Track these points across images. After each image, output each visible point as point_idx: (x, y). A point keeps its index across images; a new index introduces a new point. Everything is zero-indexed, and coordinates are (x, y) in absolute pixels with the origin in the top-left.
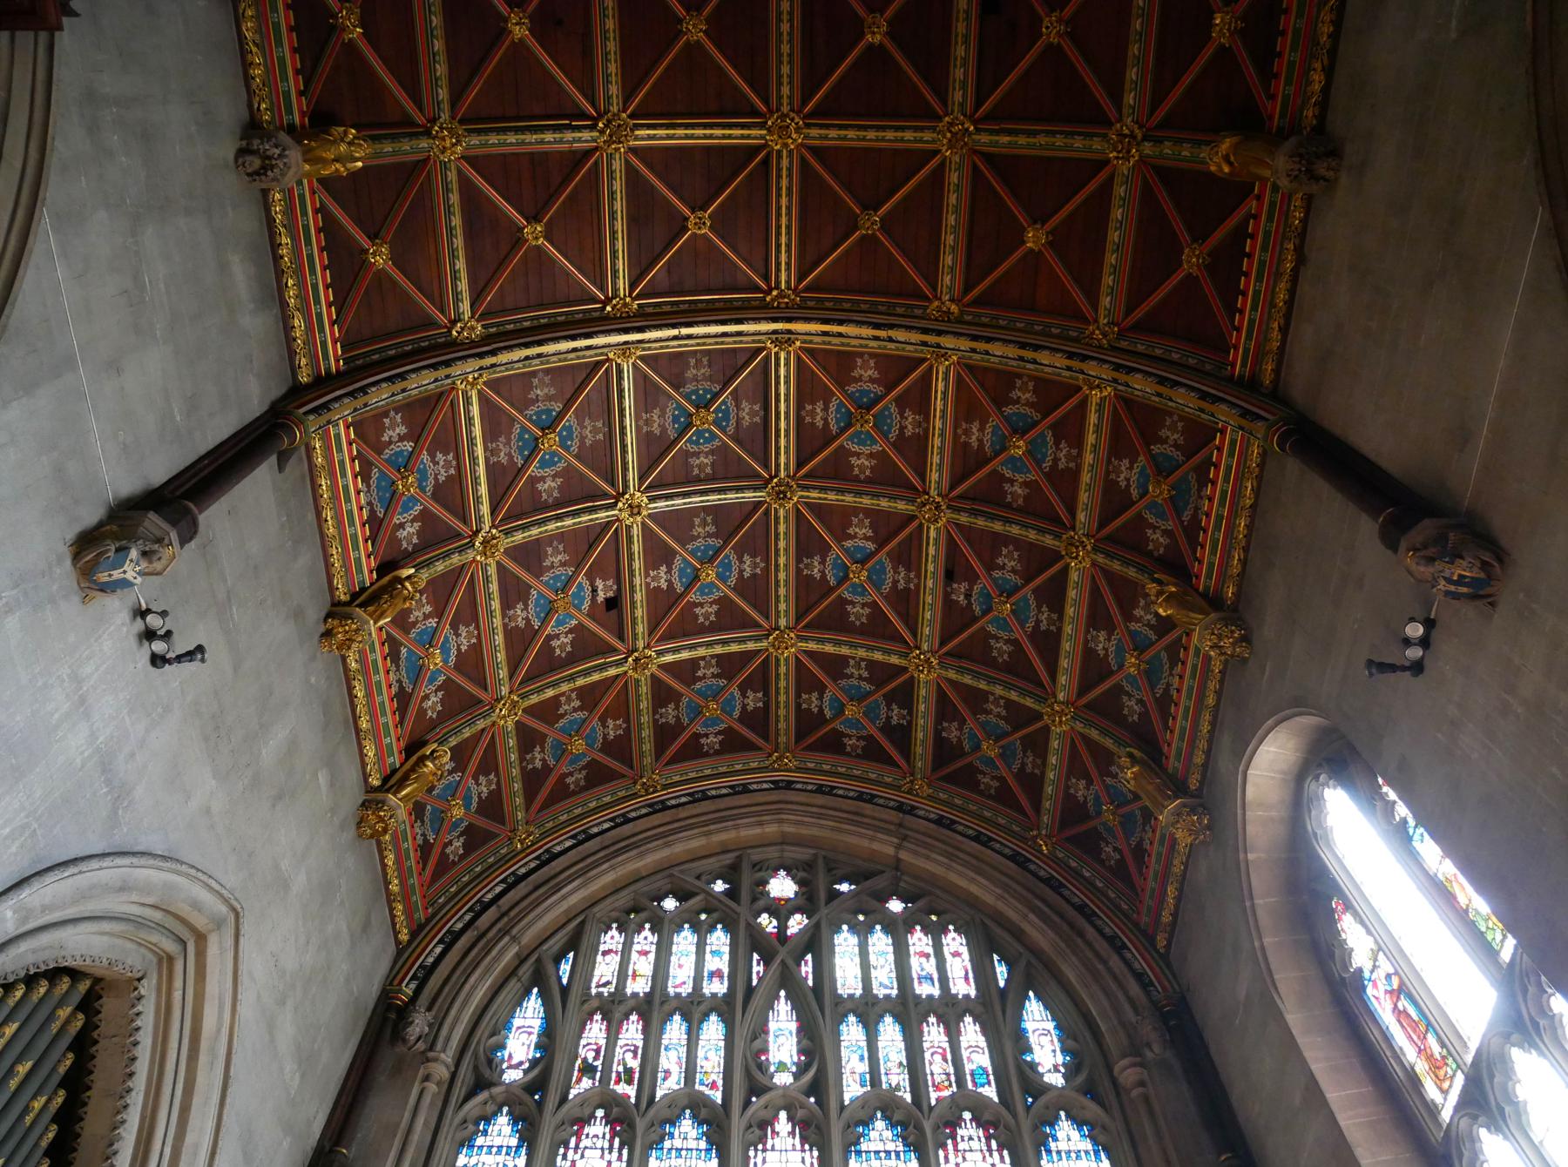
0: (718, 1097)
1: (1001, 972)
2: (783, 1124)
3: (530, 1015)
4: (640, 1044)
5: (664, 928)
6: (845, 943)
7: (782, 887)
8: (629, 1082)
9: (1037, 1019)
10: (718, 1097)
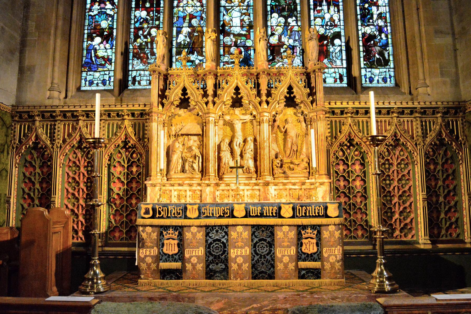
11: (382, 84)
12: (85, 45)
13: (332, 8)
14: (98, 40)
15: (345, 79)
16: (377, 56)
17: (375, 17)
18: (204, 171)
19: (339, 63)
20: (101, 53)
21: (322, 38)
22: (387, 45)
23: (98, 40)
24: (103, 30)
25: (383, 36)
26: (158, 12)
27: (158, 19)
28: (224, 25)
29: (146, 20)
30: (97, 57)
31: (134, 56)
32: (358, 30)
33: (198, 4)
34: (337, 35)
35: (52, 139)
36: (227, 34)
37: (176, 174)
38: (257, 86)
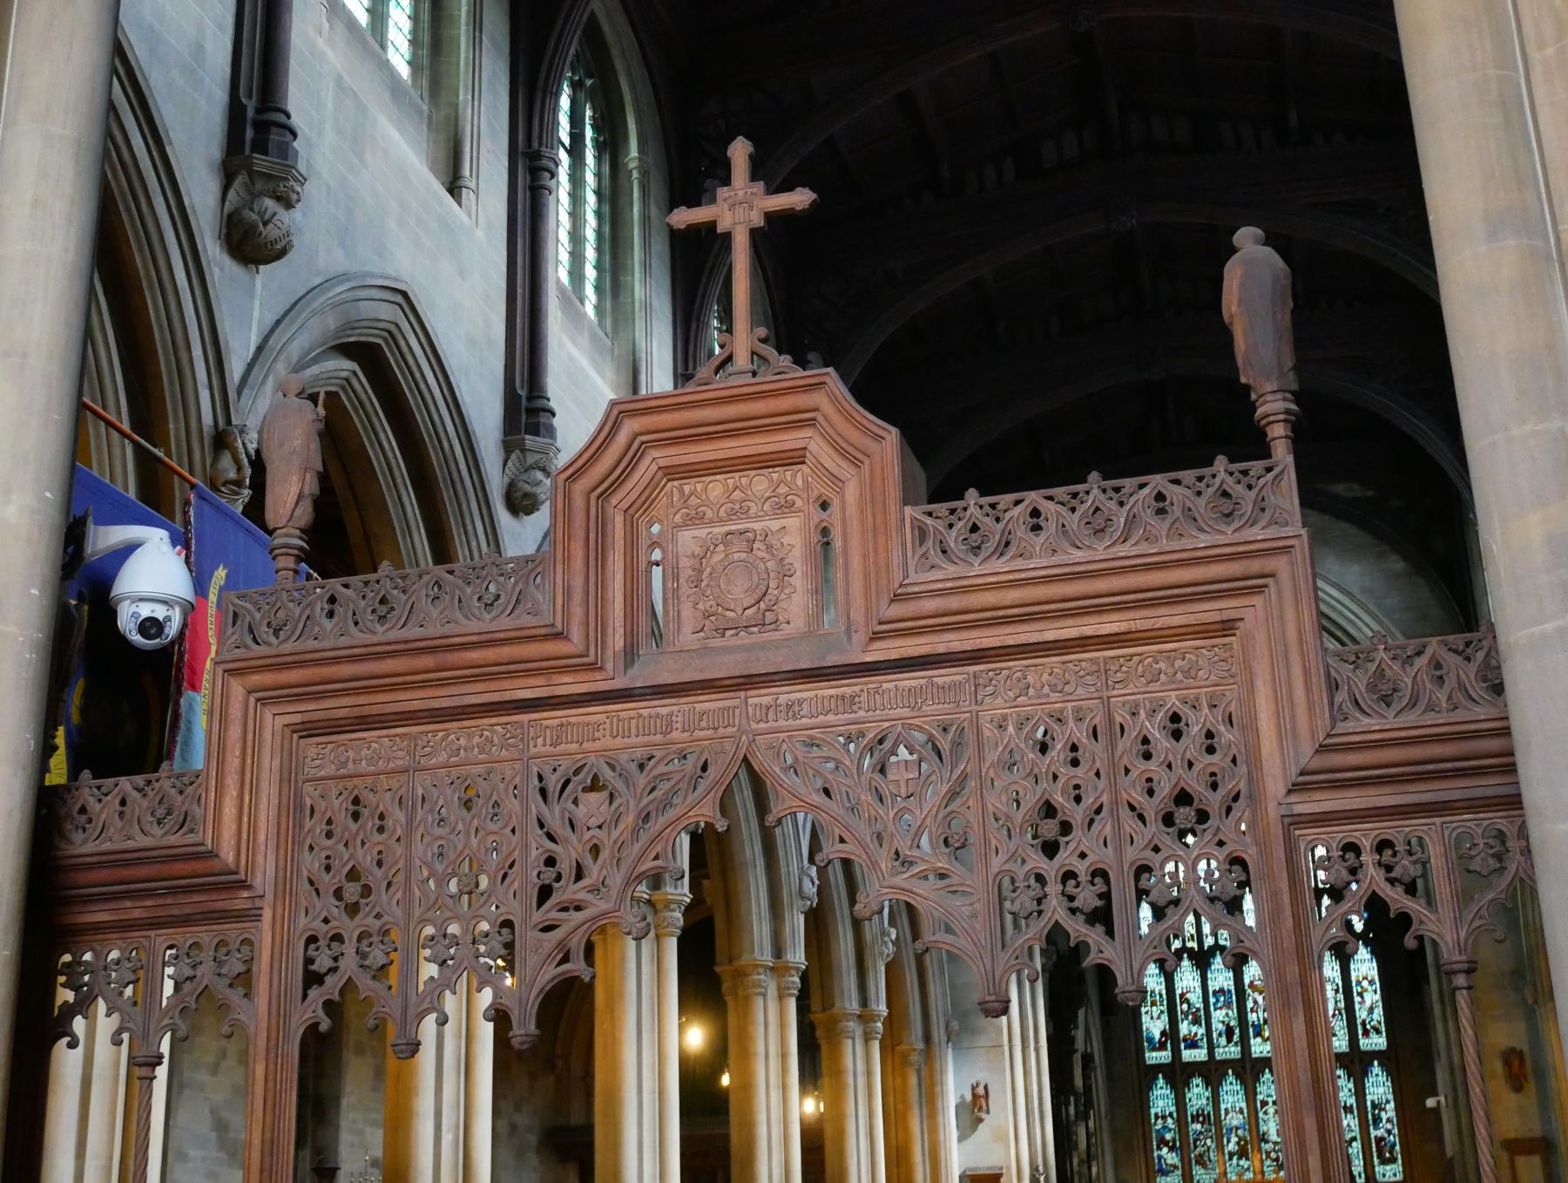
4: (1194, 922)
8: (1193, 940)
11: (1393, 1179)
12: (1155, 1154)
13: (1349, 1116)
14: (1165, 1150)
15: (1363, 1175)
16: (1388, 1155)
17: (1384, 1121)
19: (1357, 1162)
20: (1169, 1162)
22: (1395, 1145)
23: (1165, 1150)
24: (1168, 1142)
25: (1392, 1137)
26: (1210, 1124)
27: (1211, 1131)
28: (1264, 1134)
29: (1201, 1133)
30: (1166, 1165)
31: (1196, 1163)
32: (1369, 1134)
33: (1241, 1117)
36: (1267, 1142)
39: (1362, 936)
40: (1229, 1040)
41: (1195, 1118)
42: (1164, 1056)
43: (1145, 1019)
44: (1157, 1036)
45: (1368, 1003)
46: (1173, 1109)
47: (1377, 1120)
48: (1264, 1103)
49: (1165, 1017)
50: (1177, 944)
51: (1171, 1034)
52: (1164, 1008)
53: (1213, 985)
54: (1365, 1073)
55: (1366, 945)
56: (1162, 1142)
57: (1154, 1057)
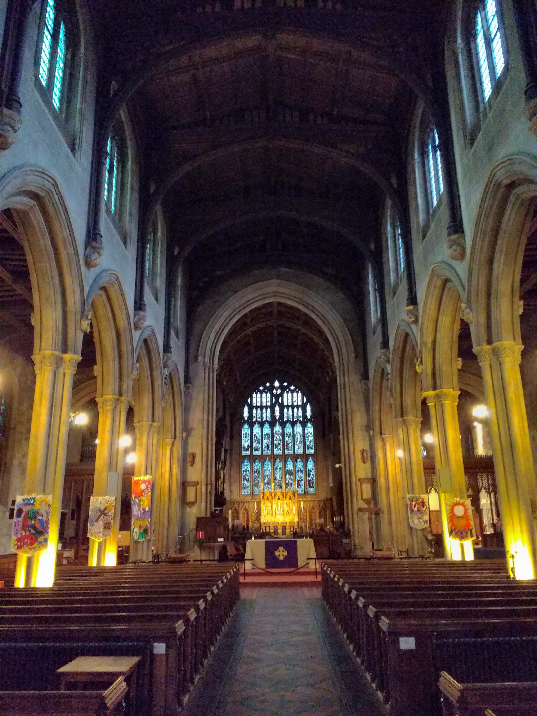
0: (270, 420)
1: (305, 399)
2: (277, 424)
3: (246, 409)
5: (261, 392)
6: (285, 395)
7: (277, 384)
9: (309, 408)
10: (270, 420)
18: (272, 514)
21: (298, 481)
34: (302, 480)
35: (239, 507)
37: (267, 515)
38: (283, 495)
39: (310, 420)
40: (268, 449)
41: (256, 472)
42: (248, 453)
43: (243, 441)
44: (246, 447)
45: (309, 440)
46: (249, 469)
47: (309, 475)
48: (277, 468)
49: (249, 441)
50: (254, 420)
51: (251, 446)
52: (249, 438)
53: (264, 432)
54: (307, 460)
55: (310, 423)
56: (245, 479)
57: (244, 453)
